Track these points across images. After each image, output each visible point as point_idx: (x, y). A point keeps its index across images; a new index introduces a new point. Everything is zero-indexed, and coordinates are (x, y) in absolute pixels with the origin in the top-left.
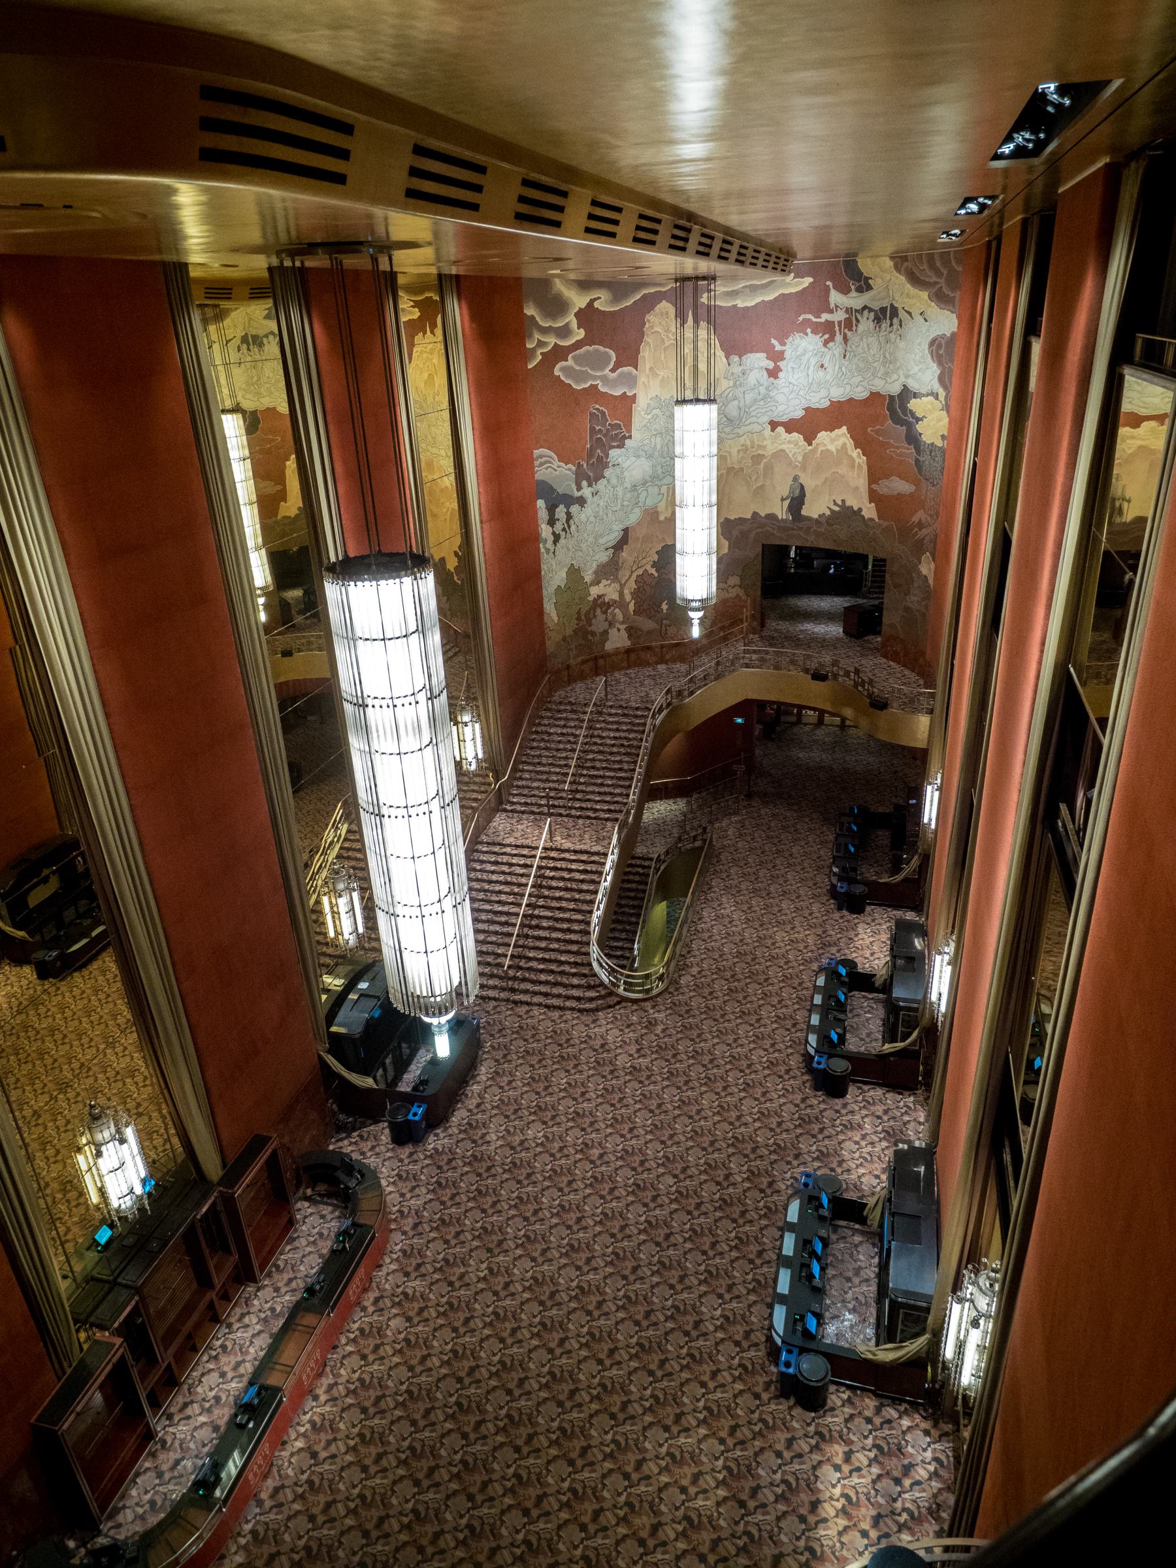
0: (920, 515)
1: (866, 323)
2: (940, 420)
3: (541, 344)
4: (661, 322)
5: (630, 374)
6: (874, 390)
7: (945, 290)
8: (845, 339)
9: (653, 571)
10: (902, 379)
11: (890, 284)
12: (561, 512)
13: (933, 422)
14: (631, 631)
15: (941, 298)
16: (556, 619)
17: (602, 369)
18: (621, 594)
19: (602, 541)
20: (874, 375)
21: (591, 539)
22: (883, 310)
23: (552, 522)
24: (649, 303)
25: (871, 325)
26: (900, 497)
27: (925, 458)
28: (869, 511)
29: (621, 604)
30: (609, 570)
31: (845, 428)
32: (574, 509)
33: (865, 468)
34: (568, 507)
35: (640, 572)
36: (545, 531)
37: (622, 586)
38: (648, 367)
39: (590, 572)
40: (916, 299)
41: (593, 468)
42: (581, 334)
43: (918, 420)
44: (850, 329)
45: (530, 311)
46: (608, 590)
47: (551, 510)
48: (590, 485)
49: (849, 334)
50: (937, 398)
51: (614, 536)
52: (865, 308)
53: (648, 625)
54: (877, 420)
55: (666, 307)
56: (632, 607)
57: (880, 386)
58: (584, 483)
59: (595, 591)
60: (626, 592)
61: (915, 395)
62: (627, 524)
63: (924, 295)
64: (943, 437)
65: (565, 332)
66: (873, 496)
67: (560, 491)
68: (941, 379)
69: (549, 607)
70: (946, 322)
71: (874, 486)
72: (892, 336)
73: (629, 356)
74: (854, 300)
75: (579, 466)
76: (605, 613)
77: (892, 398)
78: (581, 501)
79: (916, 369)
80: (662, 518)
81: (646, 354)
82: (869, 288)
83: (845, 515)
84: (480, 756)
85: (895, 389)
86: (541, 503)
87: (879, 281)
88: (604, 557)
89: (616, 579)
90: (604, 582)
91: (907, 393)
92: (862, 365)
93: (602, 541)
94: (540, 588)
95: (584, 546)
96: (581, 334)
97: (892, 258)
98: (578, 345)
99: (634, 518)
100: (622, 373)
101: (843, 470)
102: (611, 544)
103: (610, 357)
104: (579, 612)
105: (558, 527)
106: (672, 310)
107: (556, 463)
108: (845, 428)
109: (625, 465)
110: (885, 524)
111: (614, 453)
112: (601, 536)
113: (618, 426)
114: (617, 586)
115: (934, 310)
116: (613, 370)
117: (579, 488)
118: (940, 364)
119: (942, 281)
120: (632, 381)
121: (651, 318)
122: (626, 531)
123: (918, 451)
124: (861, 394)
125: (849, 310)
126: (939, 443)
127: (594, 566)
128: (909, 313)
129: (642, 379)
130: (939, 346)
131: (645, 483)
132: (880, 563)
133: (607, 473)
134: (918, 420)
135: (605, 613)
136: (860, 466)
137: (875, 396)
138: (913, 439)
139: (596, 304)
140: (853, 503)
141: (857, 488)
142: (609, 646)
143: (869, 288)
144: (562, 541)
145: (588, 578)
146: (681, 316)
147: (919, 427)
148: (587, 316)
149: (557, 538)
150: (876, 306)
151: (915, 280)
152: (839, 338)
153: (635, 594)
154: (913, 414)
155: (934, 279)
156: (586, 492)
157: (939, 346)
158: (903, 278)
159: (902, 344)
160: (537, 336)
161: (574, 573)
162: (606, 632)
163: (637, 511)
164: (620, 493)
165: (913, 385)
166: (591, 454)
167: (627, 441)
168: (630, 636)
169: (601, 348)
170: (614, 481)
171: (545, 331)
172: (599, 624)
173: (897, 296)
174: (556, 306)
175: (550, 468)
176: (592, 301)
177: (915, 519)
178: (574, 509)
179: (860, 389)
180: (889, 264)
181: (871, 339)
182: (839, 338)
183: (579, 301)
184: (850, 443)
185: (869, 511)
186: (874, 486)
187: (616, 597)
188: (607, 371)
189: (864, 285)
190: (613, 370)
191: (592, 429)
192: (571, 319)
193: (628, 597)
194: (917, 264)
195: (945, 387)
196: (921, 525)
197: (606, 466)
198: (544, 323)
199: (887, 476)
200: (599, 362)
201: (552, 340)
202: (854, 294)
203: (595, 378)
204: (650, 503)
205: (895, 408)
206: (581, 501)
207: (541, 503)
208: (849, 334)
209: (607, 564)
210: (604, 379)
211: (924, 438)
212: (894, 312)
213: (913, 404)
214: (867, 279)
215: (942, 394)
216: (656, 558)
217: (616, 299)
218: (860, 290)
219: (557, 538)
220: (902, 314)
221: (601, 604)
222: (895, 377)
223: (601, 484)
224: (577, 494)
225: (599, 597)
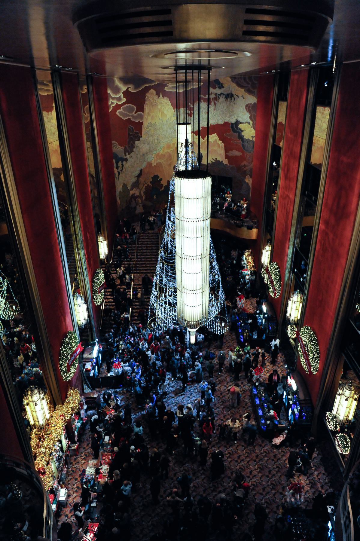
0: (245, 163)
1: (222, 99)
2: (251, 131)
3: (112, 103)
5: (141, 114)
6: (226, 121)
7: (251, 89)
8: (215, 104)
9: (150, 185)
10: (236, 118)
11: (231, 87)
12: (120, 163)
13: (249, 132)
14: (144, 206)
15: (249, 92)
16: (120, 203)
17: (132, 112)
18: (140, 193)
19: (134, 174)
20: (226, 116)
22: (228, 95)
23: (117, 168)
24: (147, 89)
25: (224, 99)
26: (237, 157)
27: (245, 144)
28: (226, 162)
29: (140, 197)
30: (136, 185)
31: (216, 134)
32: (124, 163)
33: (223, 147)
34: (122, 162)
35: (146, 185)
36: (116, 171)
37: (141, 190)
40: (241, 91)
41: (130, 148)
42: (124, 100)
43: (242, 131)
44: (217, 101)
45: (109, 91)
46: (135, 192)
47: (117, 163)
49: (216, 102)
50: (249, 123)
51: (138, 172)
52: (222, 94)
53: (149, 204)
54: (229, 132)
55: (152, 91)
56: (144, 198)
57: (228, 120)
58: (127, 153)
59: (132, 192)
60: (142, 192)
61: (241, 123)
62: (142, 168)
63: (243, 90)
64: (252, 137)
65: (119, 99)
66: (227, 157)
67: (120, 156)
68: (251, 118)
69: (118, 199)
70: (252, 100)
71: (227, 154)
72: (232, 103)
73: (141, 108)
74: (218, 91)
75: (125, 147)
76: (135, 200)
77: (232, 124)
78: (126, 160)
79: (241, 114)
80: (153, 166)
81: (146, 107)
82: (223, 87)
83: (217, 163)
84: (107, 253)
85: (234, 121)
86: (114, 161)
87: (226, 85)
88: (134, 180)
89: (138, 188)
90: (134, 189)
91: (237, 123)
92: (221, 113)
93: (134, 174)
94: (115, 192)
95: (128, 176)
96: (124, 100)
97: (231, 78)
99: (144, 166)
100: (138, 114)
101: (215, 148)
102: (137, 175)
104: (127, 201)
105: (120, 169)
106: (155, 92)
107: (118, 146)
108: (216, 134)
109: (140, 147)
110: (232, 166)
111: (136, 142)
112: (133, 172)
113: (137, 133)
114: (138, 190)
115: (246, 95)
116: (135, 113)
117: (126, 155)
118: (250, 113)
119: (249, 86)
120: (142, 117)
122: (141, 170)
123: (243, 141)
124: (221, 122)
125: (216, 94)
126: (251, 139)
127: (131, 183)
128: (238, 96)
129: (145, 116)
130: (249, 107)
131: (147, 153)
132: (231, 179)
133: (134, 150)
134: (242, 131)
135: (135, 200)
136: (222, 147)
137: (226, 123)
138: (241, 137)
139: (129, 90)
140: (219, 159)
141: (221, 154)
142: (137, 212)
143: (223, 87)
144: (121, 174)
145: (129, 188)
146: (158, 95)
147: (243, 133)
148: (126, 93)
149: (119, 173)
150: (226, 93)
151: (240, 85)
152: (213, 103)
153: (145, 193)
154: (240, 129)
155: (246, 85)
156: (128, 156)
157: (249, 107)
158: (235, 85)
159: (235, 106)
160: (111, 100)
161: (125, 186)
162: (135, 208)
163: (145, 163)
165: (240, 120)
166: (129, 143)
167: (141, 138)
168: (144, 208)
169: (131, 105)
170: (137, 152)
171: (113, 98)
172: (133, 204)
173: (233, 90)
174: (117, 90)
175: (118, 149)
176: (128, 88)
177: (243, 164)
179: (221, 121)
180: (230, 79)
181: (224, 104)
182: (213, 103)
183: (124, 88)
184: (218, 139)
185: (226, 162)
186: (227, 154)
187: (138, 194)
188: (133, 113)
189: (221, 86)
190: (135, 113)
191: (129, 134)
193: (142, 194)
194: (242, 80)
195: (252, 121)
196: (245, 166)
197: (134, 147)
198: (113, 96)
199: (232, 150)
200: (131, 110)
201: (115, 102)
202: (217, 89)
203: (129, 116)
204: (149, 160)
205: (235, 127)
206: (126, 160)
207: (114, 161)
208: (216, 102)
209: (135, 182)
211: (245, 137)
212: (232, 95)
213: (240, 126)
214: (222, 84)
215: (251, 123)
216: (151, 180)
217: (136, 88)
218: (219, 88)
219: (119, 173)
220: (235, 96)
221: (134, 197)
222: (233, 117)
223: (133, 153)
224: (125, 157)
225: (133, 194)
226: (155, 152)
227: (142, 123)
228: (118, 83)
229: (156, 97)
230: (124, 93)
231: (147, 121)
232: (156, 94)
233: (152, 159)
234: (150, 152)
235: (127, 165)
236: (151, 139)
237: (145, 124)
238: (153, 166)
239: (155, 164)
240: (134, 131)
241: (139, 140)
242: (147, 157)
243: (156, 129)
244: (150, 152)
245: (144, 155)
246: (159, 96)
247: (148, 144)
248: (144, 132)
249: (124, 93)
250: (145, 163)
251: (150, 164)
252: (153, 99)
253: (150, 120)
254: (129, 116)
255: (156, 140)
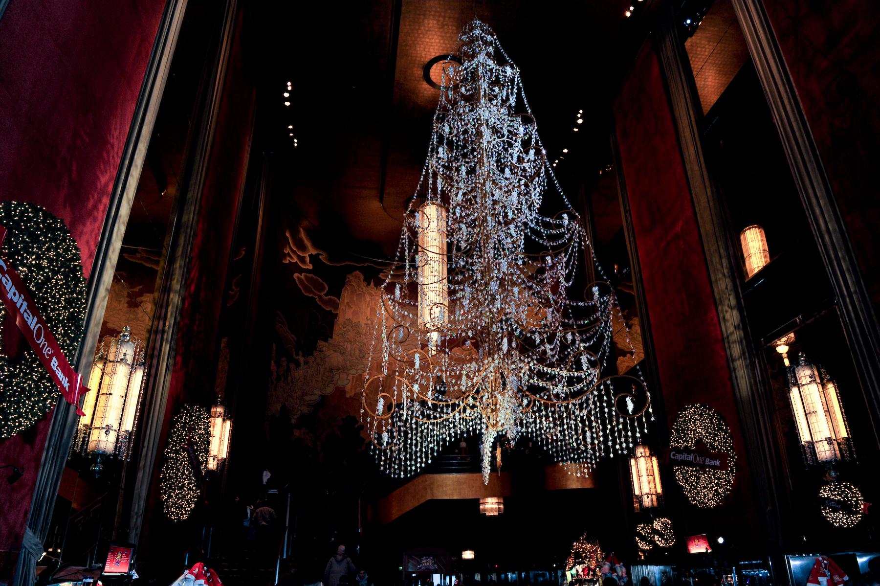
4: (356, 279)
19: (307, 398)
21: (299, 393)
24: (350, 270)
32: (292, 366)
38: (346, 301)
39: (296, 417)
48: (303, 356)
51: (314, 397)
58: (301, 353)
65: (302, 259)
73: (336, 290)
80: (348, 396)
81: (346, 295)
93: (307, 398)
96: (311, 267)
98: (307, 271)
99: (329, 390)
100: (330, 299)
103: (324, 289)
106: (362, 277)
111: (320, 343)
116: (326, 295)
117: (297, 355)
120: (336, 306)
121: (350, 277)
145: (293, 421)
148: (314, 259)
156: (302, 359)
164: (322, 370)
170: (319, 360)
176: (318, 255)
178: (292, 366)
188: (322, 294)
190: (326, 295)
192: (307, 255)
203: (316, 295)
204: (340, 383)
206: (298, 365)
210: (320, 297)
223: (311, 359)
226: (353, 371)
227: (336, 316)
228: (303, 235)
229: (363, 284)
230: (311, 256)
231: (345, 314)
232: (365, 280)
233: (345, 381)
234: (343, 369)
235: (299, 373)
236: (349, 346)
237: (341, 319)
238: (348, 396)
239: (352, 394)
240: (319, 325)
241: (326, 341)
242: (336, 377)
243: (359, 333)
244: (343, 369)
245: (331, 370)
246: (369, 284)
247: (343, 354)
248: (338, 329)
249: (311, 256)
250: (331, 385)
251: (340, 392)
252: (359, 286)
253: (349, 315)
254: (316, 295)
255: (357, 352)
